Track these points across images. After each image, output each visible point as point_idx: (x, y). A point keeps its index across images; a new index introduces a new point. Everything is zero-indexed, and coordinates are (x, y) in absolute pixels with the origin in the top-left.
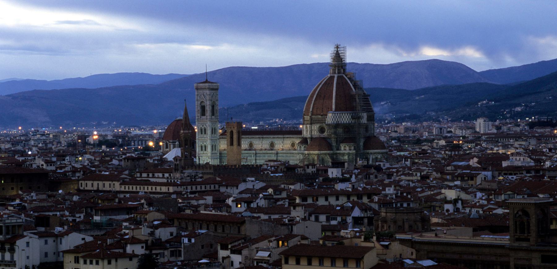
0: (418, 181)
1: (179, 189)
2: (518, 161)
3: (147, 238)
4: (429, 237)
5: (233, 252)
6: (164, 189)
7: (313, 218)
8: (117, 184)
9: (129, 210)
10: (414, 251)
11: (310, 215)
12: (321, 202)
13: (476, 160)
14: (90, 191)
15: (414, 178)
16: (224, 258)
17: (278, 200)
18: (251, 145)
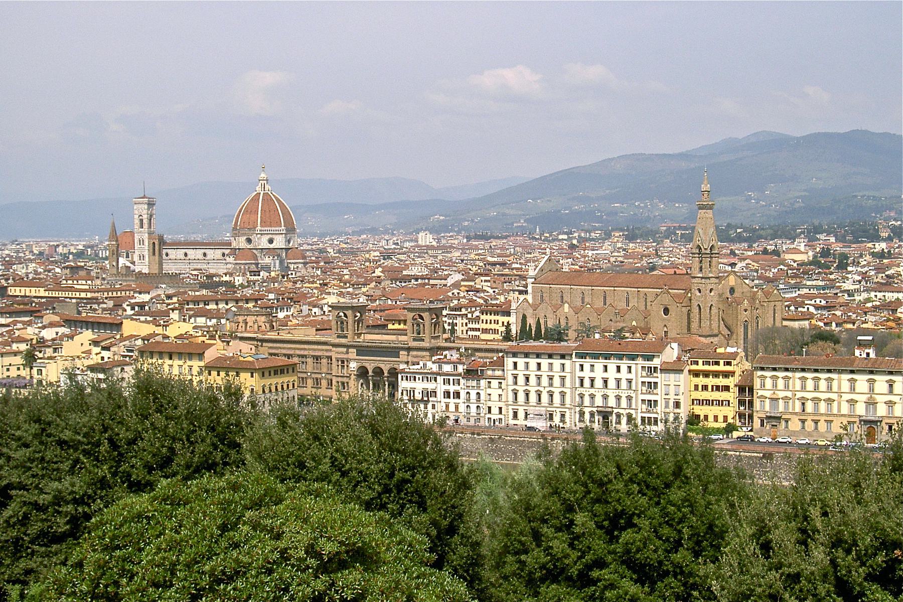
0: (316, 288)
1: (96, 295)
2: (414, 271)
3: (32, 337)
4: (272, 335)
5: (104, 348)
6: (83, 295)
7: (192, 320)
8: (42, 290)
9: (31, 313)
10: (254, 348)
11: (190, 318)
12: (212, 306)
13: (380, 269)
14: (17, 296)
15: (315, 285)
16: (97, 354)
17: (169, 304)
18: (186, 255)
